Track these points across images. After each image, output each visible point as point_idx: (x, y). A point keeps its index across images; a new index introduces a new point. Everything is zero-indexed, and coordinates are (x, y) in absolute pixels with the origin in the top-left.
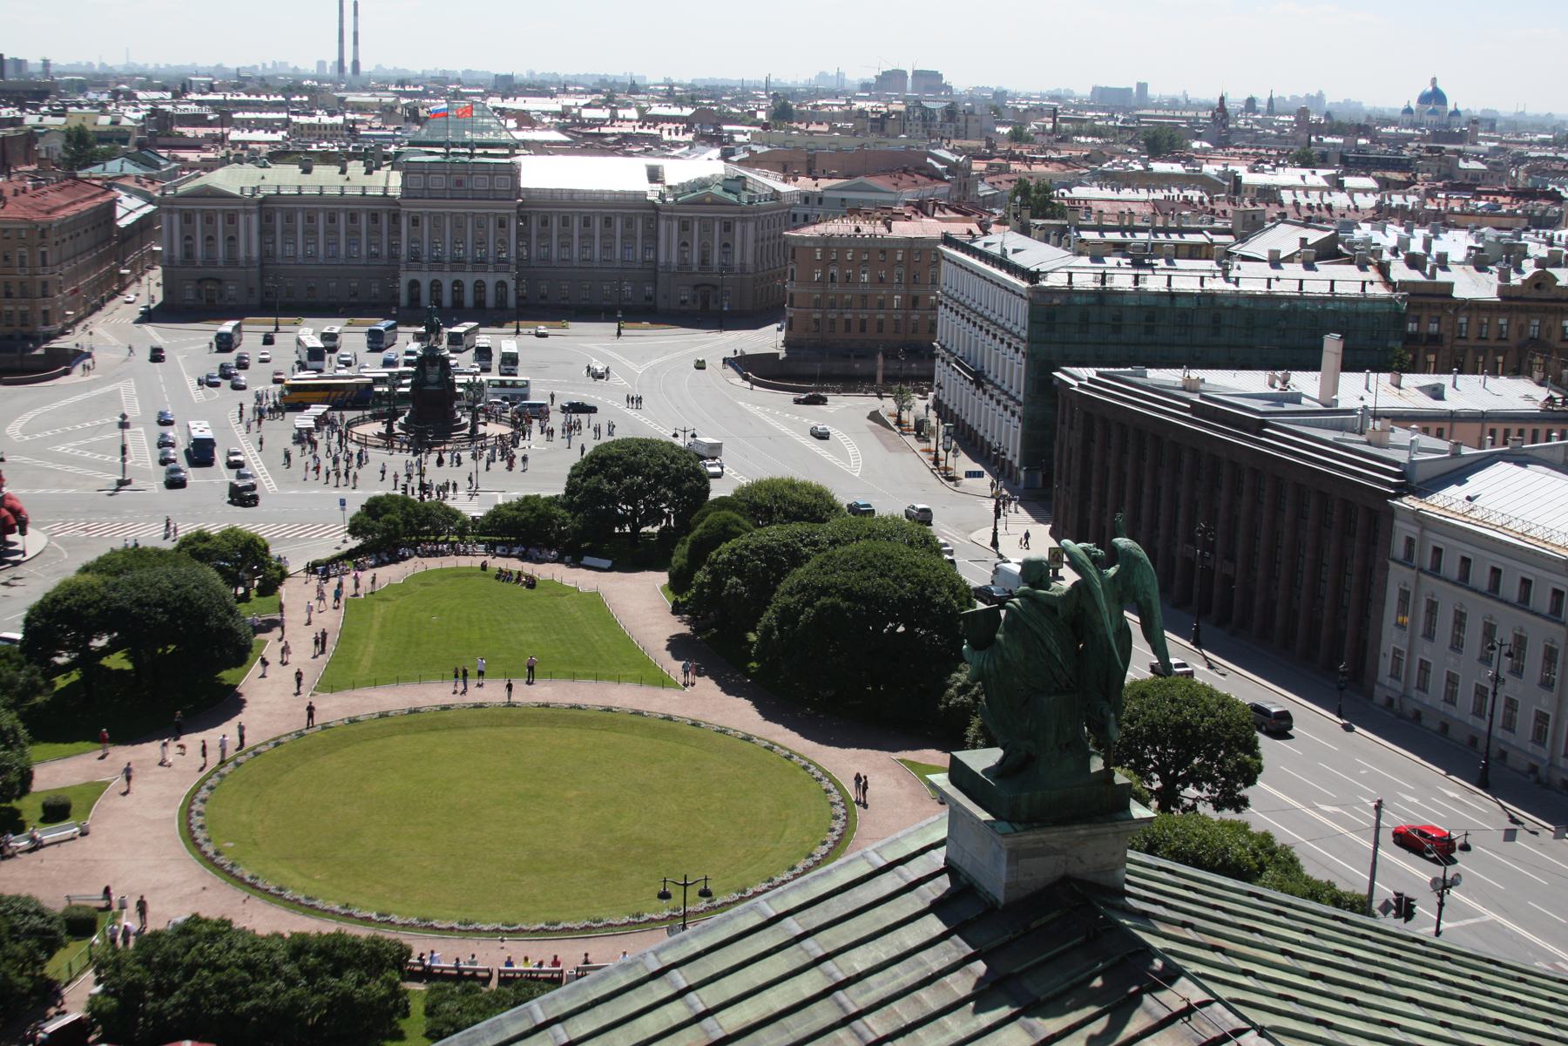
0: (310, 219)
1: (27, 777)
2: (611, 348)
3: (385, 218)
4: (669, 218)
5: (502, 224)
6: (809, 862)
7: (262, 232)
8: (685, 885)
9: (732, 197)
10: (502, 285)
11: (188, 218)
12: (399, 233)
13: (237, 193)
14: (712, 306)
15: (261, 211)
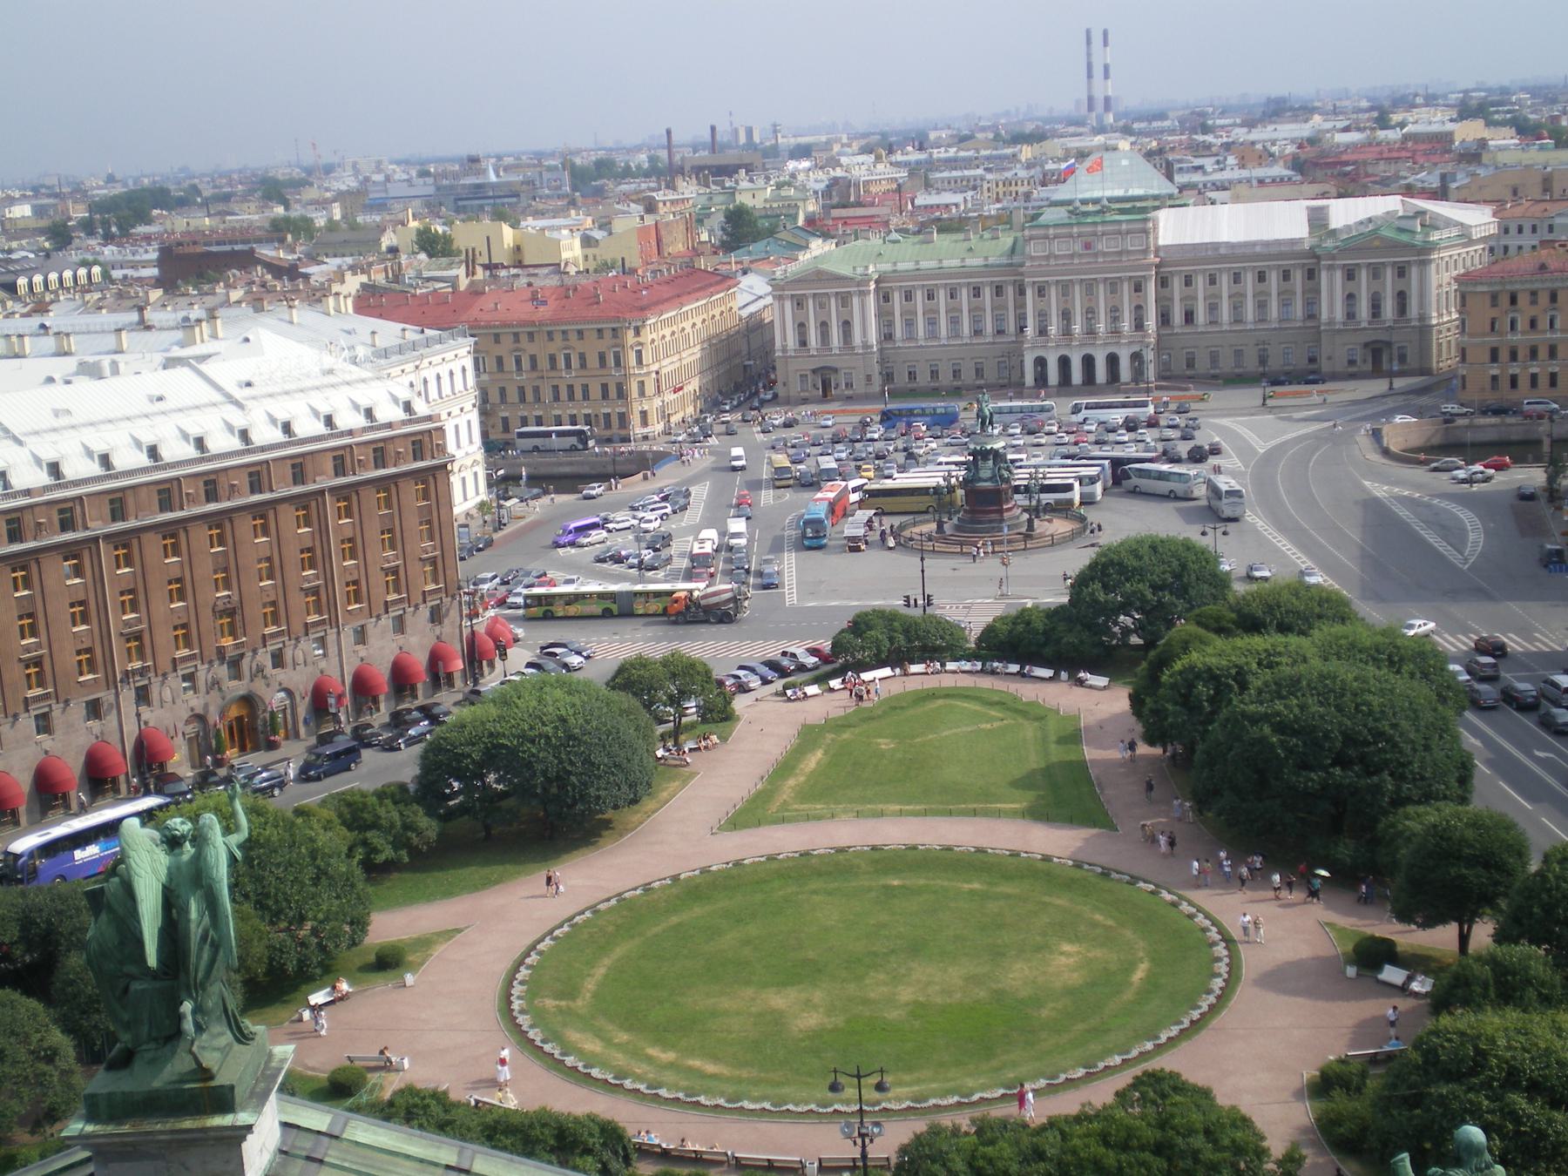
0: (931, 296)
1: (360, 924)
2: (1241, 423)
3: (1010, 291)
4: (1330, 268)
5: (1138, 288)
6: (1149, 1046)
7: (879, 315)
8: (859, 1077)
9: (1404, 238)
10: (1136, 357)
11: (799, 303)
12: (1024, 305)
13: (845, 271)
14: (1385, 366)
15: (877, 289)
